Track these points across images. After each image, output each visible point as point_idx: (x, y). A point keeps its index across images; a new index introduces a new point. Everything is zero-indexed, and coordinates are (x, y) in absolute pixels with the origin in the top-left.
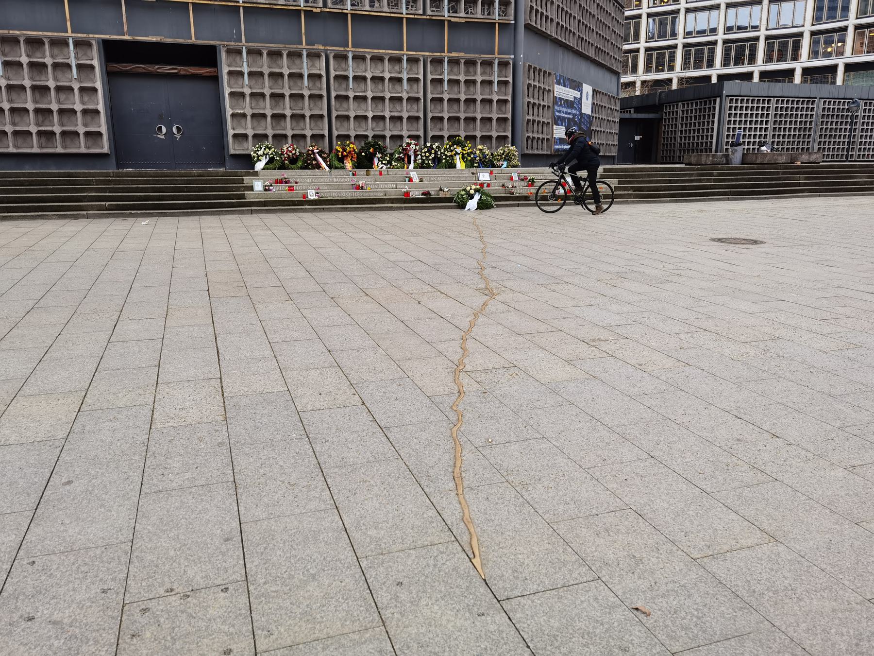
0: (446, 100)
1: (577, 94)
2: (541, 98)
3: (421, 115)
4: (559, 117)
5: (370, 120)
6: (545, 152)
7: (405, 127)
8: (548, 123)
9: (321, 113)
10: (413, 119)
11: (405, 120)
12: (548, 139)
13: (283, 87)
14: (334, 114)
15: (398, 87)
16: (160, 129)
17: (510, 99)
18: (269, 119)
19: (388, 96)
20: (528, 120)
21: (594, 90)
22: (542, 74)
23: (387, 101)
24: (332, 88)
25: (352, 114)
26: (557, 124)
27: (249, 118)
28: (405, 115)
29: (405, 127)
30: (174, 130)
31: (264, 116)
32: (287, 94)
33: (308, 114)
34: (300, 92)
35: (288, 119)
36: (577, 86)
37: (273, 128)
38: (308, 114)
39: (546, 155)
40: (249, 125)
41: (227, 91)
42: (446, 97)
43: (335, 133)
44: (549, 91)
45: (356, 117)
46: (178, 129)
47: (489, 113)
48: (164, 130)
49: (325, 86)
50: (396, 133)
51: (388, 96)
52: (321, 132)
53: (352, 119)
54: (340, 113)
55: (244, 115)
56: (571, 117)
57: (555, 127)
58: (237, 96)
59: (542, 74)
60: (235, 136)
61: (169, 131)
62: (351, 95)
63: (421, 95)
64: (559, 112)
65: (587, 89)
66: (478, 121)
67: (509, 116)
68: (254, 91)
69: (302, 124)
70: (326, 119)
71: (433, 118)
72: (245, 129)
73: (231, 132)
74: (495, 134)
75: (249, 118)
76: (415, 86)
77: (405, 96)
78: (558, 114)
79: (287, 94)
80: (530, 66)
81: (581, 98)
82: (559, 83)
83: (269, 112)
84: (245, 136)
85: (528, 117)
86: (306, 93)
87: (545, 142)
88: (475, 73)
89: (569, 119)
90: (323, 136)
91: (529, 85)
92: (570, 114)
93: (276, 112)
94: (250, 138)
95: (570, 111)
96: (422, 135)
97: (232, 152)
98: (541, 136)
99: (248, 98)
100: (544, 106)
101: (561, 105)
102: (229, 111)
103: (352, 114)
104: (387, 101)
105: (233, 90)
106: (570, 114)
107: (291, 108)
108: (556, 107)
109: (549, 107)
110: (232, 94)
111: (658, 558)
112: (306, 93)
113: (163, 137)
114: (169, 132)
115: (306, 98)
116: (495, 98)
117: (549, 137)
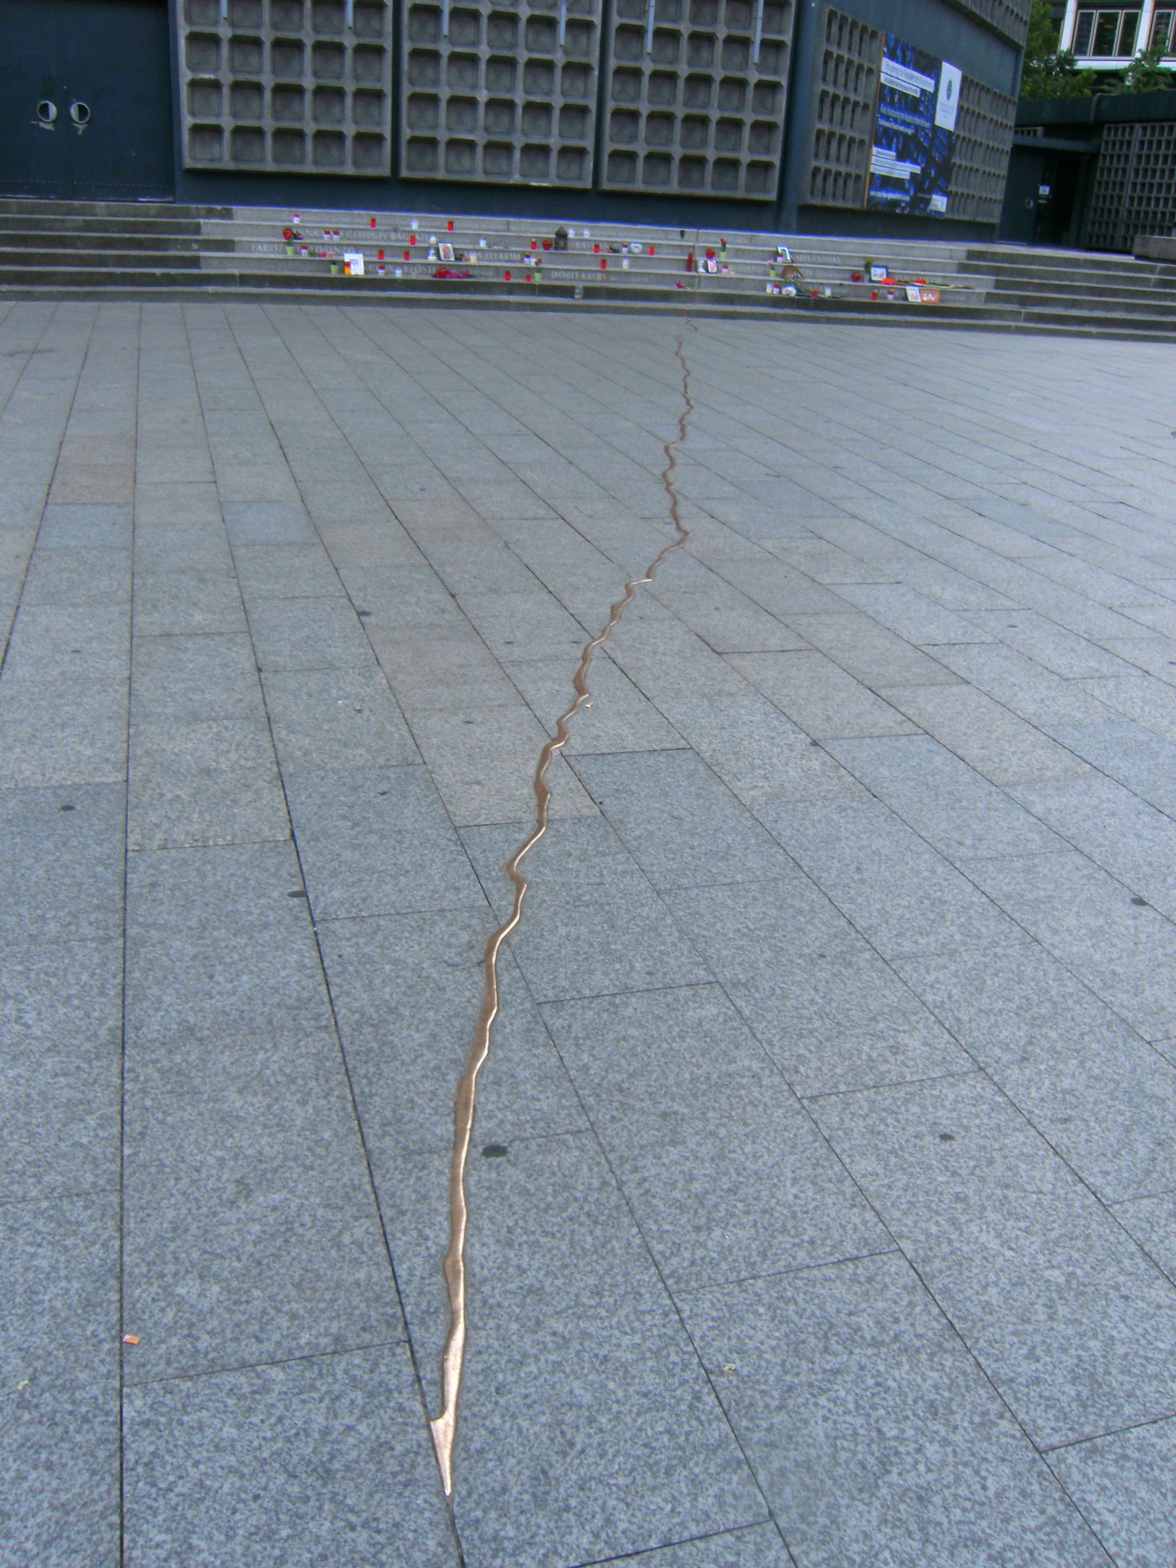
0: (647, 73)
1: (928, 84)
2: (851, 85)
3: (592, 104)
4: (886, 130)
5: (481, 110)
6: (849, 205)
7: (555, 129)
8: (862, 142)
9: (377, 86)
10: (573, 112)
11: (556, 114)
12: (858, 177)
13: (300, 27)
14: (406, 91)
15: (545, 39)
16: (45, 110)
17: (784, 82)
18: (268, 95)
19: (523, 56)
20: (820, 133)
21: (964, 79)
22: (857, 33)
23: (521, 69)
24: (405, 32)
25: (445, 93)
26: (878, 144)
27: (226, 91)
28: (558, 102)
29: (555, 129)
30: (74, 112)
31: (258, 88)
32: (309, 42)
33: (350, 88)
34: (337, 39)
35: (308, 97)
36: (931, 68)
37: (276, 116)
38: (350, 88)
39: (853, 212)
40: (226, 108)
41: (183, 30)
42: (648, 67)
43: (407, 133)
44: (870, 71)
45: (454, 101)
46: (82, 111)
47: (666, 145)
48: (53, 110)
49: (389, 28)
50: (535, 140)
51: (523, 56)
52: (377, 130)
53: (443, 105)
54: (418, 90)
55: (216, 85)
56: (910, 132)
57: (875, 150)
58: (204, 41)
59: (857, 33)
60: (197, 129)
61: (63, 114)
62: (445, 50)
63: (594, 60)
64: (887, 118)
65: (951, 74)
66: (713, 127)
67: (780, 119)
68: (241, 32)
69: (336, 110)
70: (388, 102)
71: (617, 113)
72: (218, 115)
73: (188, 121)
74: (745, 157)
75: (226, 91)
76: (583, 39)
77: (559, 58)
78: (883, 123)
79: (309, 42)
80: (832, 14)
81: (935, 95)
82: (892, 56)
83: (268, 81)
84: (216, 130)
85: (819, 126)
86: (349, 42)
87: (851, 183)
88: (714, 20)
89: (905, 135)
90: (379, 138)
91: (828, 54)
92: (908, 125)
93: (283, 80)
94: (227, 136)
95: (909, 119)
96: (591, 149)
97: (188, 163)
98: (843, 169)
99: (225, 50)
100: (856, 104)
101: (892, 105)
102: (186, 76)
103: (445, 93)
104: (521, 69)
105: (196, 29)
106: (908, 125)
107: (315, 74)
108: (883, 110)
109: (866, 107)
110: (193, 38)
111: (945, 1442)
112: (349, 42)
113: (50, 127)
114: (63, 114)
115: (349, 54)
116: (753, 77)
117: (861, 172)
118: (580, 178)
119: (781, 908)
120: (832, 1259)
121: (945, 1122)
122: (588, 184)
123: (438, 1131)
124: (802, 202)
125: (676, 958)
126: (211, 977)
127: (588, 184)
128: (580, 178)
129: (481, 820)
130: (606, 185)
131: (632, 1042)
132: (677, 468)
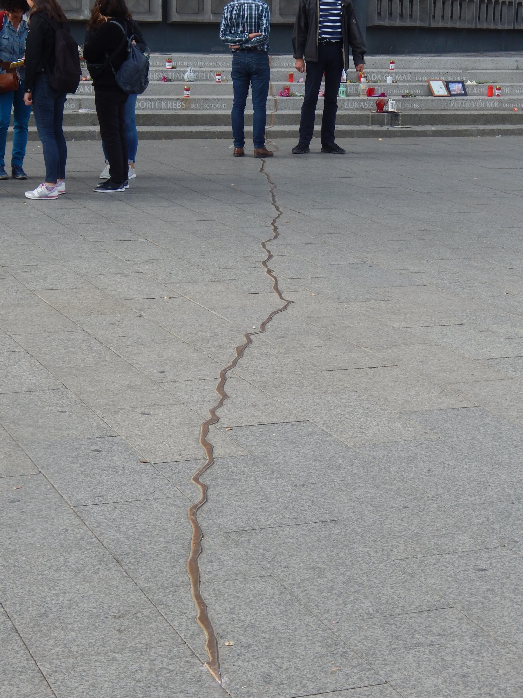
6: (418, 24)
118: (149, 12)
119: (377, 489)
120: (415, 611)
121: (482, 565)
122: (158, 17)
123: (180, 579)
124: (370, 24)
125: (312, 512)
126: (16, 531)
127: (158, 17)
128: (149, 12)
129: (169, 459)
130: (175, 17)
131: (289, 544)
132: (274, 259)
